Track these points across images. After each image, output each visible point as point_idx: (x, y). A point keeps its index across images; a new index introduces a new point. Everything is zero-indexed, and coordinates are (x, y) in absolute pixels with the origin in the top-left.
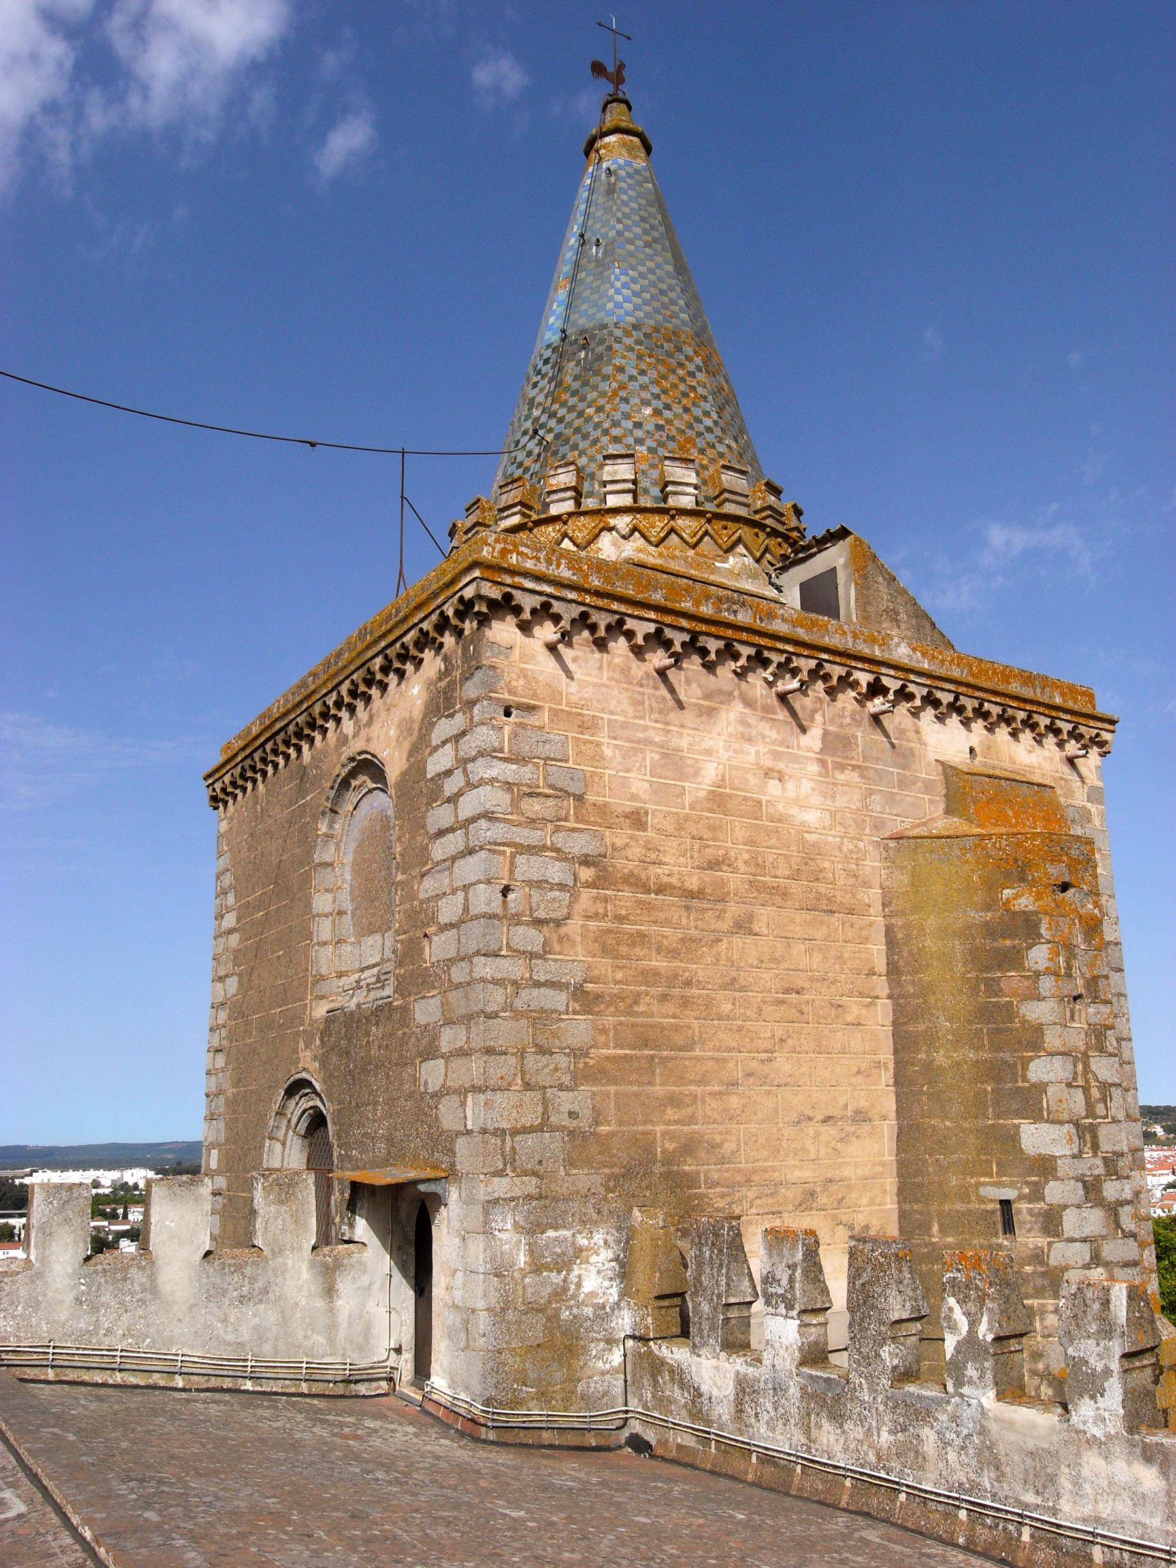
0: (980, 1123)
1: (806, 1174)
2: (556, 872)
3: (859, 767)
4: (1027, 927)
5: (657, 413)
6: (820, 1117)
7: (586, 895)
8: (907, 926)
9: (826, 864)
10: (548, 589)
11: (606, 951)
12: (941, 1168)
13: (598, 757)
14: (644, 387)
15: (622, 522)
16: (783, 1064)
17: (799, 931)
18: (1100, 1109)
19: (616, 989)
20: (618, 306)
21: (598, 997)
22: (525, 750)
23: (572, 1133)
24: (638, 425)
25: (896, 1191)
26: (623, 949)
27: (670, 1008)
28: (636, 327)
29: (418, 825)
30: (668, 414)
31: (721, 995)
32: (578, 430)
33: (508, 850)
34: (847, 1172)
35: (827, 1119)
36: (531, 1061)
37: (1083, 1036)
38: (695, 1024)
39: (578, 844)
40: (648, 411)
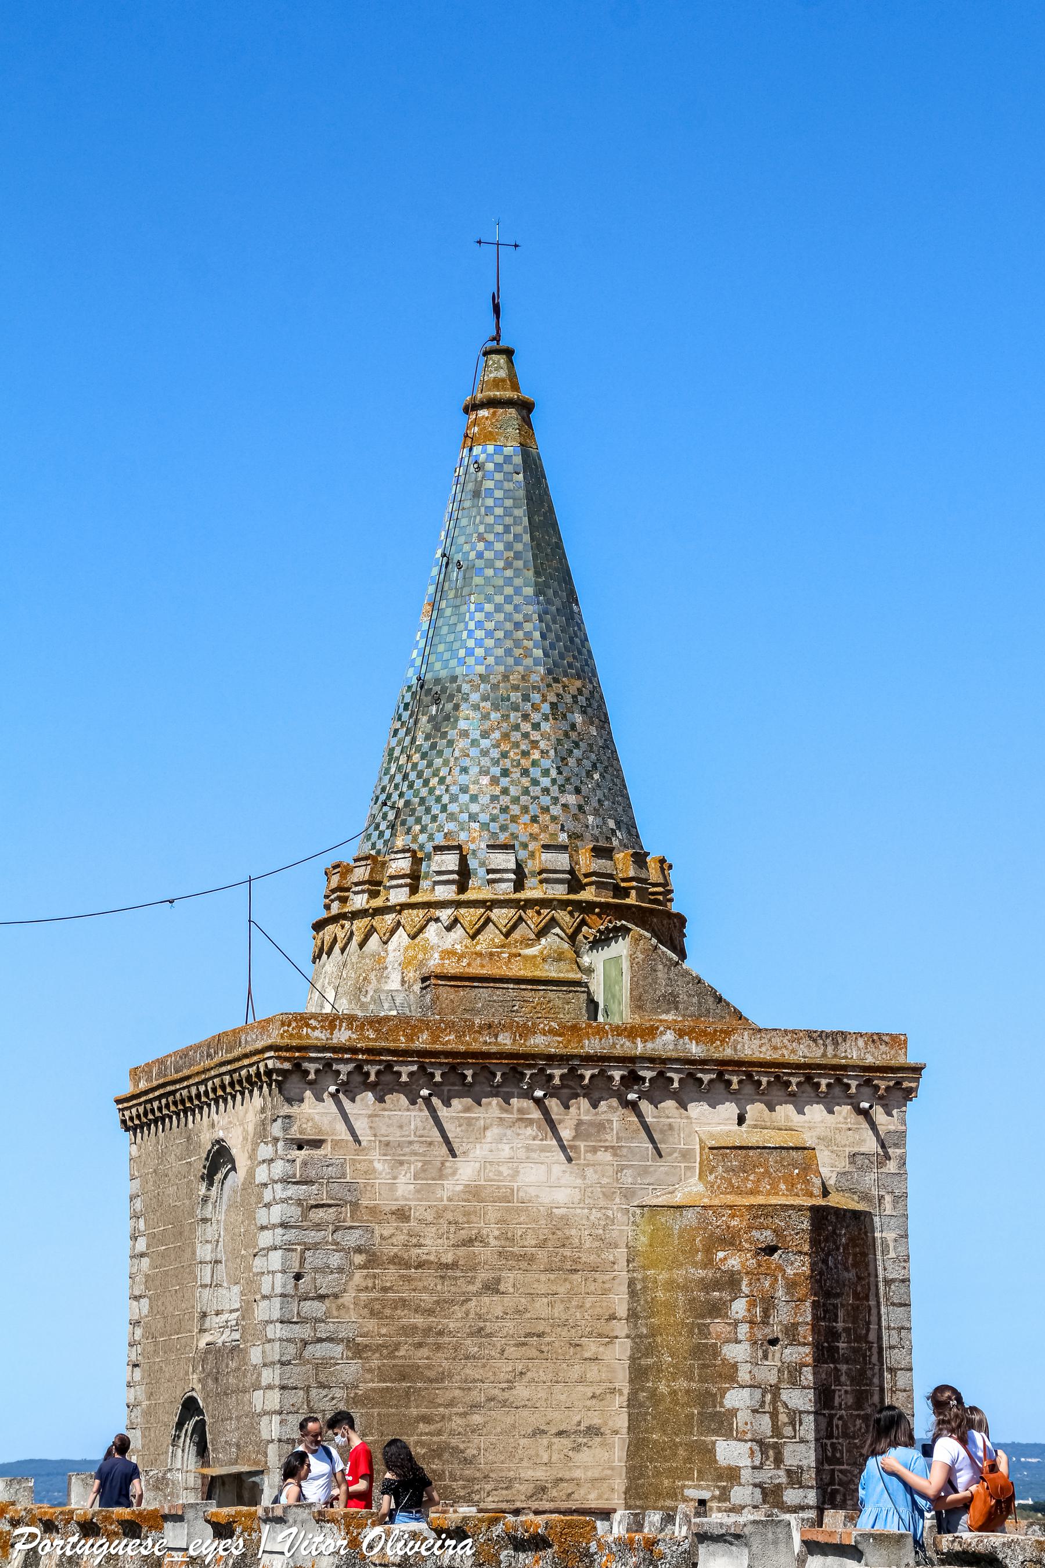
0: (685, 1439)
1: (540, 1474)
2: (336, 1260)
3: (612, 1147)
4: (731, 1282)
5: (494, 781)
6: (553, 1431)
7: (358, 1277)
8: (644, 1279)
9: (573, 1232)
10: (329, 1055)
11: (373, 1313)
12: (658, 1474)
13: (370, 1172)
14: (485, 753)
15: (445, 914)
16: (522, 1391)
17: (542, 1289)
18: (788, 1431)
22: (312, 1174)
24: (474, 798)
25: (623, 1489)
26: (388, 1312)
27: (425, 1352)
29: (251, 1216)
30: (505, 782)
31: (469, 1342)
32: (422, 801)
33: (299, 1248)
34: (578, 1474)
35: (560, 1433)
36: (314, 1392)
37: (775, 1371)
38: (445, 1363)
39: (352, 1239)
40: (485, 780)
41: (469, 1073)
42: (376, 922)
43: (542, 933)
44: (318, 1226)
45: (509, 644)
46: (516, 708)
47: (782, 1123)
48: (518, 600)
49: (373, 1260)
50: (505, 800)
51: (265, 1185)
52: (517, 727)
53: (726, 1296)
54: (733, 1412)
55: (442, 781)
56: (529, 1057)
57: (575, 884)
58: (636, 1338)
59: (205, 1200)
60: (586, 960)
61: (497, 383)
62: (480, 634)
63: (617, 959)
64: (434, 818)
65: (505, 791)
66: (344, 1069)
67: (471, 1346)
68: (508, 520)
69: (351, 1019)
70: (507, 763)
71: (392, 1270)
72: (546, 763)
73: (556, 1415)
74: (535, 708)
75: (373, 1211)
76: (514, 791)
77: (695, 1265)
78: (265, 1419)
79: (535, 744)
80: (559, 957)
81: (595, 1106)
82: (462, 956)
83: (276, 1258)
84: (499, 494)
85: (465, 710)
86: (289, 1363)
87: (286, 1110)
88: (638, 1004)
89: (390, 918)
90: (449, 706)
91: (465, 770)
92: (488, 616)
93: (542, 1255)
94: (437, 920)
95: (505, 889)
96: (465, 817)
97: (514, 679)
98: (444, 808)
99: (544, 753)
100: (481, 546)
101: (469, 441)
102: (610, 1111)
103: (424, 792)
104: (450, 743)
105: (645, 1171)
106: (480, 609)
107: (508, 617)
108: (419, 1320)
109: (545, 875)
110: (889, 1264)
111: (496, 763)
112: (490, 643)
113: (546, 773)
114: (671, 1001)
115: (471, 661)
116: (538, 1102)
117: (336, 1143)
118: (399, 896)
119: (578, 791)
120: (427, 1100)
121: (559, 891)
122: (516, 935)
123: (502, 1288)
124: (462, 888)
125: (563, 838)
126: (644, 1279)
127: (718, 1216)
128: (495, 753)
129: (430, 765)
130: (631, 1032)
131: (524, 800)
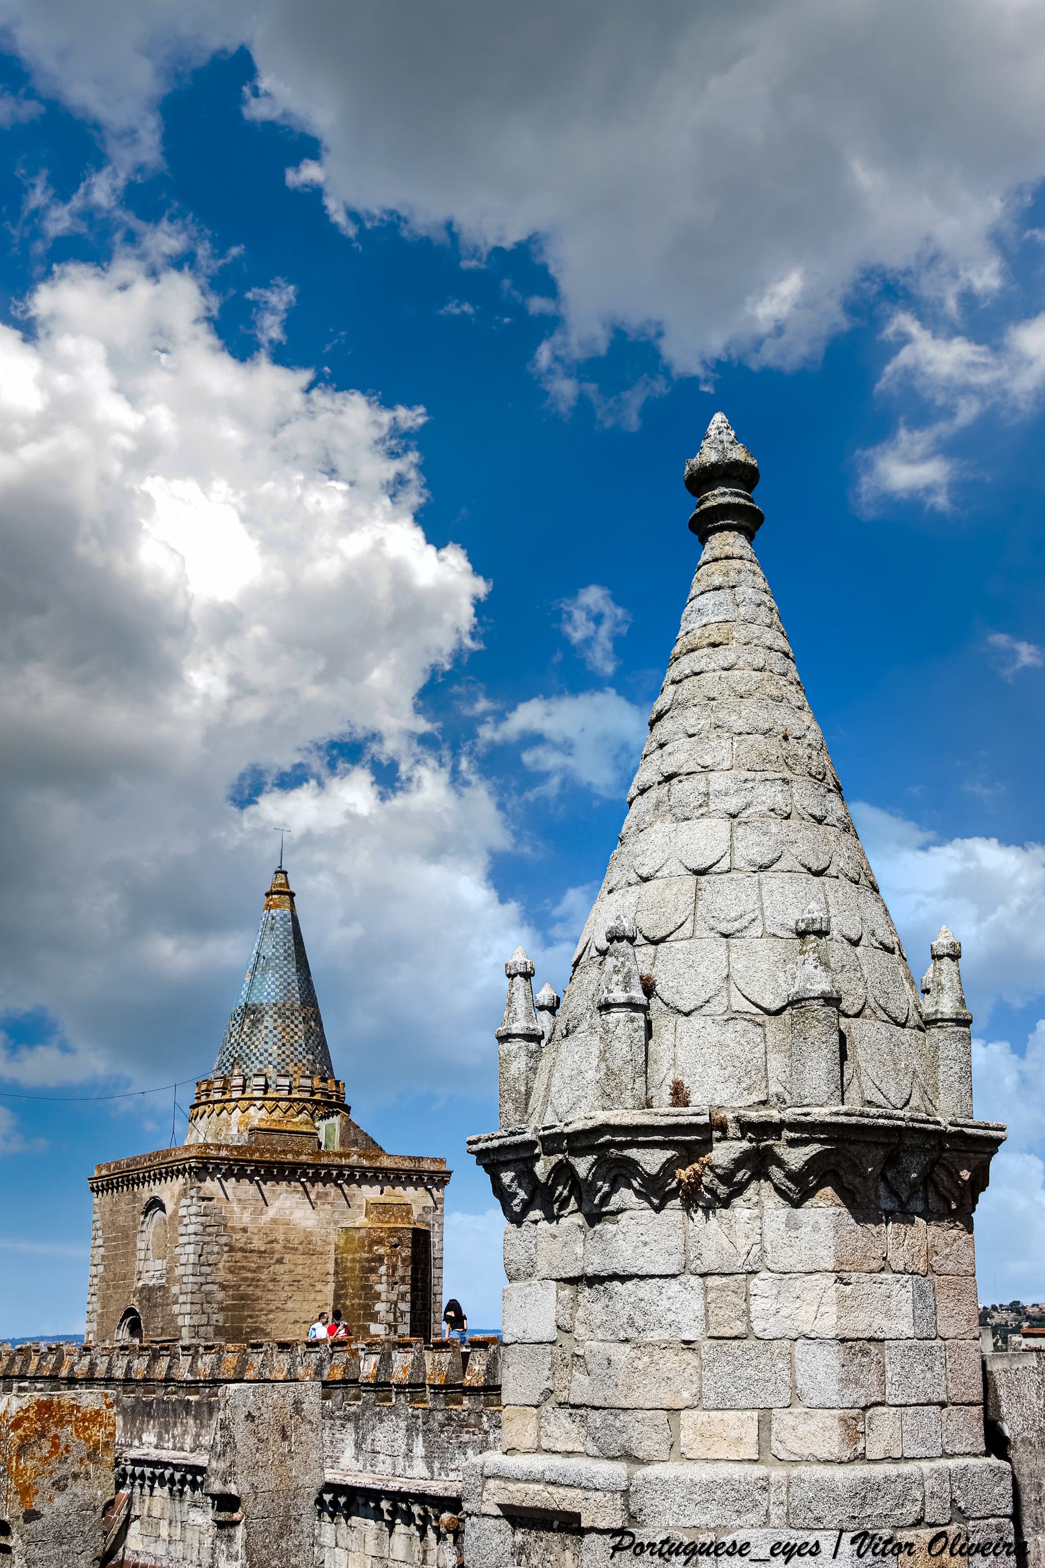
0: (357, 1324)
2: (216, 1249)
5: (279, 1048)
7: (226, 1255)
8: (342, 1258)
11: (231, 1272)
13: (232, 1212)
14: (275, 1036)
15: (259, 1103)
16: (290, 1305)
17: (300, 1262)
19: (233, 1283)
20: (269, 994)
21: (227, 1286)
22: (208, 1212)
23: (216, 1326)
24: (270, 1055)
26: (237, 1271)
27: (251, 1288)
28: (275, 1005)
30: (283, 1048)
31: (269, 1284)
32: (247, 1055)
35: (305, 1322)
36: (205, 1305)
38: (260, 1293)
39: (223, 1240)
40: (275, 1047)
41: (275, 1170)
42: (226, 1105)
43: (299, 1113)
44: (209, 1235)
45: (285, 991)
46: (288, 1018)
47: (397, 1194)
48: (289, 973)
49: (232, 1249)
50: (283, 1056)
51: (185, 1216)
52: (288, 1026)
53: (377, 1264)
54: (378, 1312)
55: (256, 1047)
56: (301, 1164)
57: (313, 1094)
58: (337, 1282)
59: (143, 1223)
60: (317, 1124)
61: (281, 885)
62: (273, 986)
63: (333, 1125)
64: (253, 1062)
65: (284, 1052)
66: (224, 1168)
67: (270, 1286)
68: (286, 941)
69: (227, 1146)
70: (284, 1041)
71: (239, 1254)
72: (301, 1042)
73: (303, 1315)
74: (296, 1018)
75: (232, 1228)
76: (287, 1052)
77: (364, 1252)
78: (180, 1318)
79: (296, 1033)
80: (307, 1123)
81: (325, 1185)
82: (268, 1121)
83: (190, 1249)
84: (281, 929)
85: (267, 1018)
86: (195, 1293)
87: (198, 1184)
88: (342, 1143)
89: (233, 1104)
90: (259, 1016)
91: (266, 1043)
92: (277, 979)
93: (300, 1247)
94: (255, 1105)
95: (284, 1094)
96: (266, 1062)
97: (287, 1006)
98: (257, 1058)
99: (300, 1037)
100: (274, 950)
101: (268, 907)
102: (331, 1188)
103: (248, 1051)
104: (260, 1031)
105: (343, 1213)
106: (273, 976)
107: (285, 980)
108: (249, 1275)
109: (301, 1088)
110: (436, 1252)
111: (280, 1040)
112: (277, 990)
113: (300, 1046)
114: (355, 1143)
115: (269, 997)
116: (302, 1183)
117: (219, 1199)
118: (236, 1095)
119: (313, 1054)
120: (257, 1182)
121: (306, 1095)
122: (288, 1113)
123: (284, 1261)
124: (266, 1092)
125: (308, 1073)
126: (342, 1258)
127: (375, 1232)
128: (280, 1037)
129: (250, 1040)
130: (340, 1155)
131: (292, 1056)
